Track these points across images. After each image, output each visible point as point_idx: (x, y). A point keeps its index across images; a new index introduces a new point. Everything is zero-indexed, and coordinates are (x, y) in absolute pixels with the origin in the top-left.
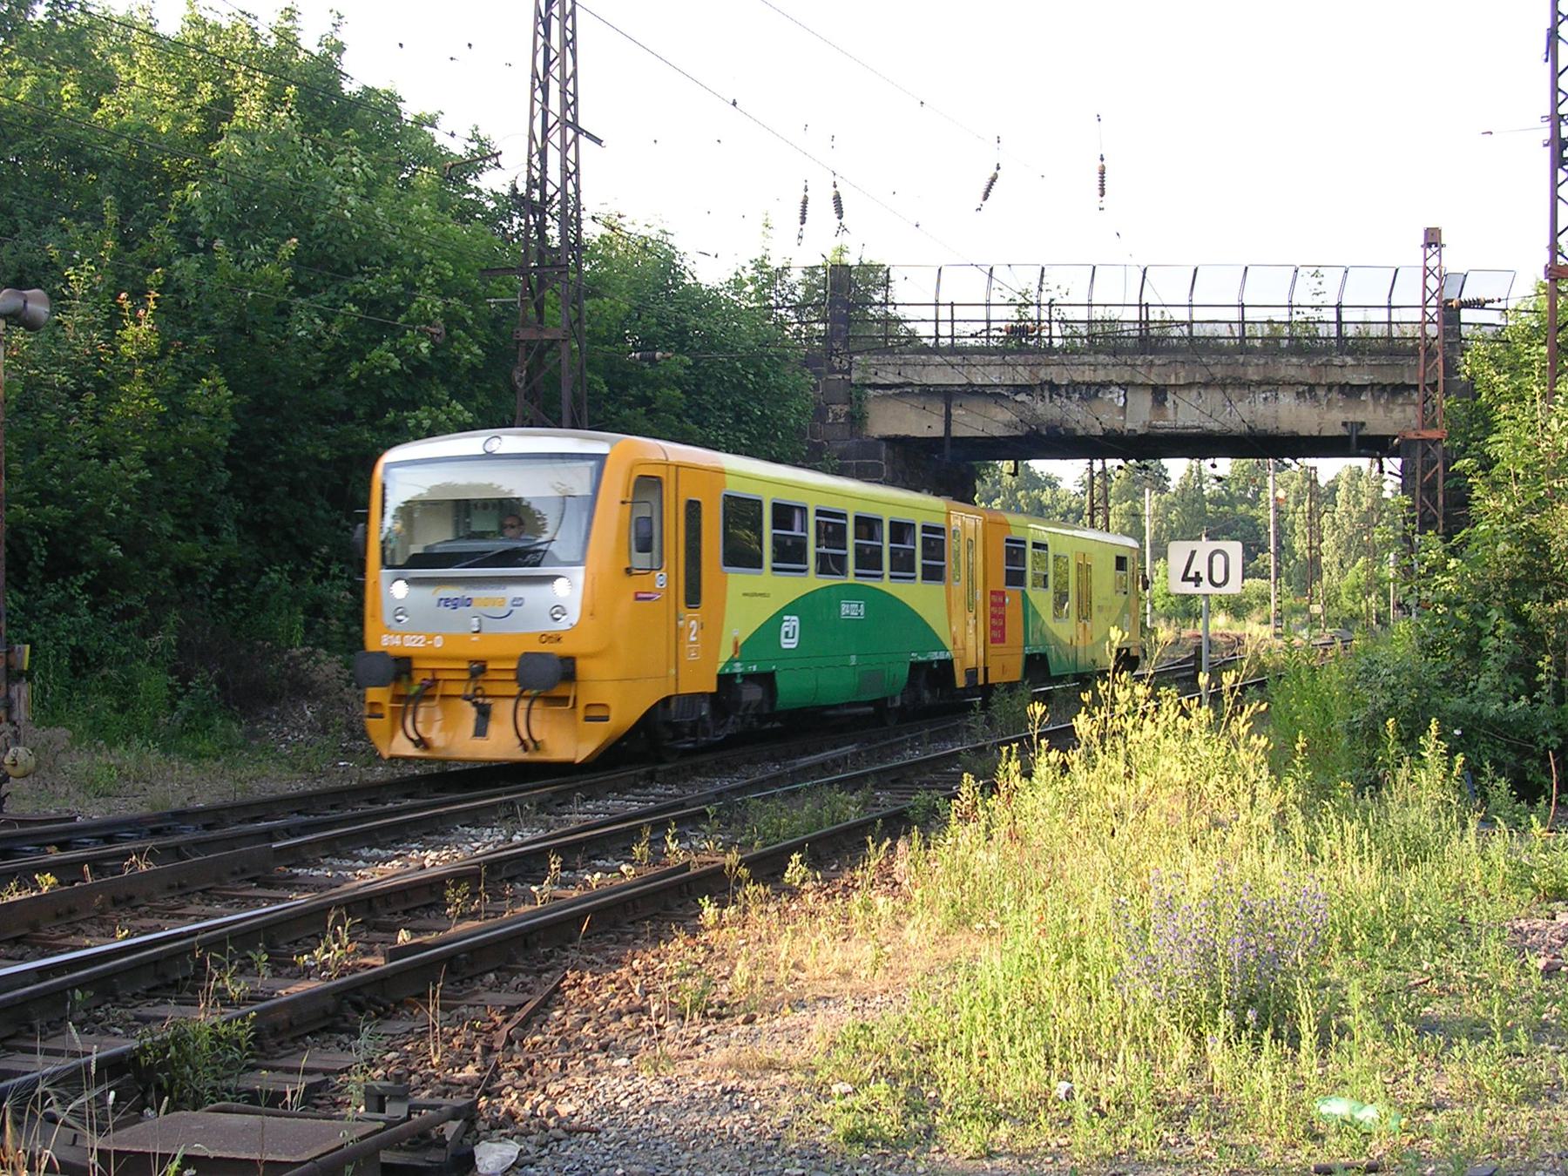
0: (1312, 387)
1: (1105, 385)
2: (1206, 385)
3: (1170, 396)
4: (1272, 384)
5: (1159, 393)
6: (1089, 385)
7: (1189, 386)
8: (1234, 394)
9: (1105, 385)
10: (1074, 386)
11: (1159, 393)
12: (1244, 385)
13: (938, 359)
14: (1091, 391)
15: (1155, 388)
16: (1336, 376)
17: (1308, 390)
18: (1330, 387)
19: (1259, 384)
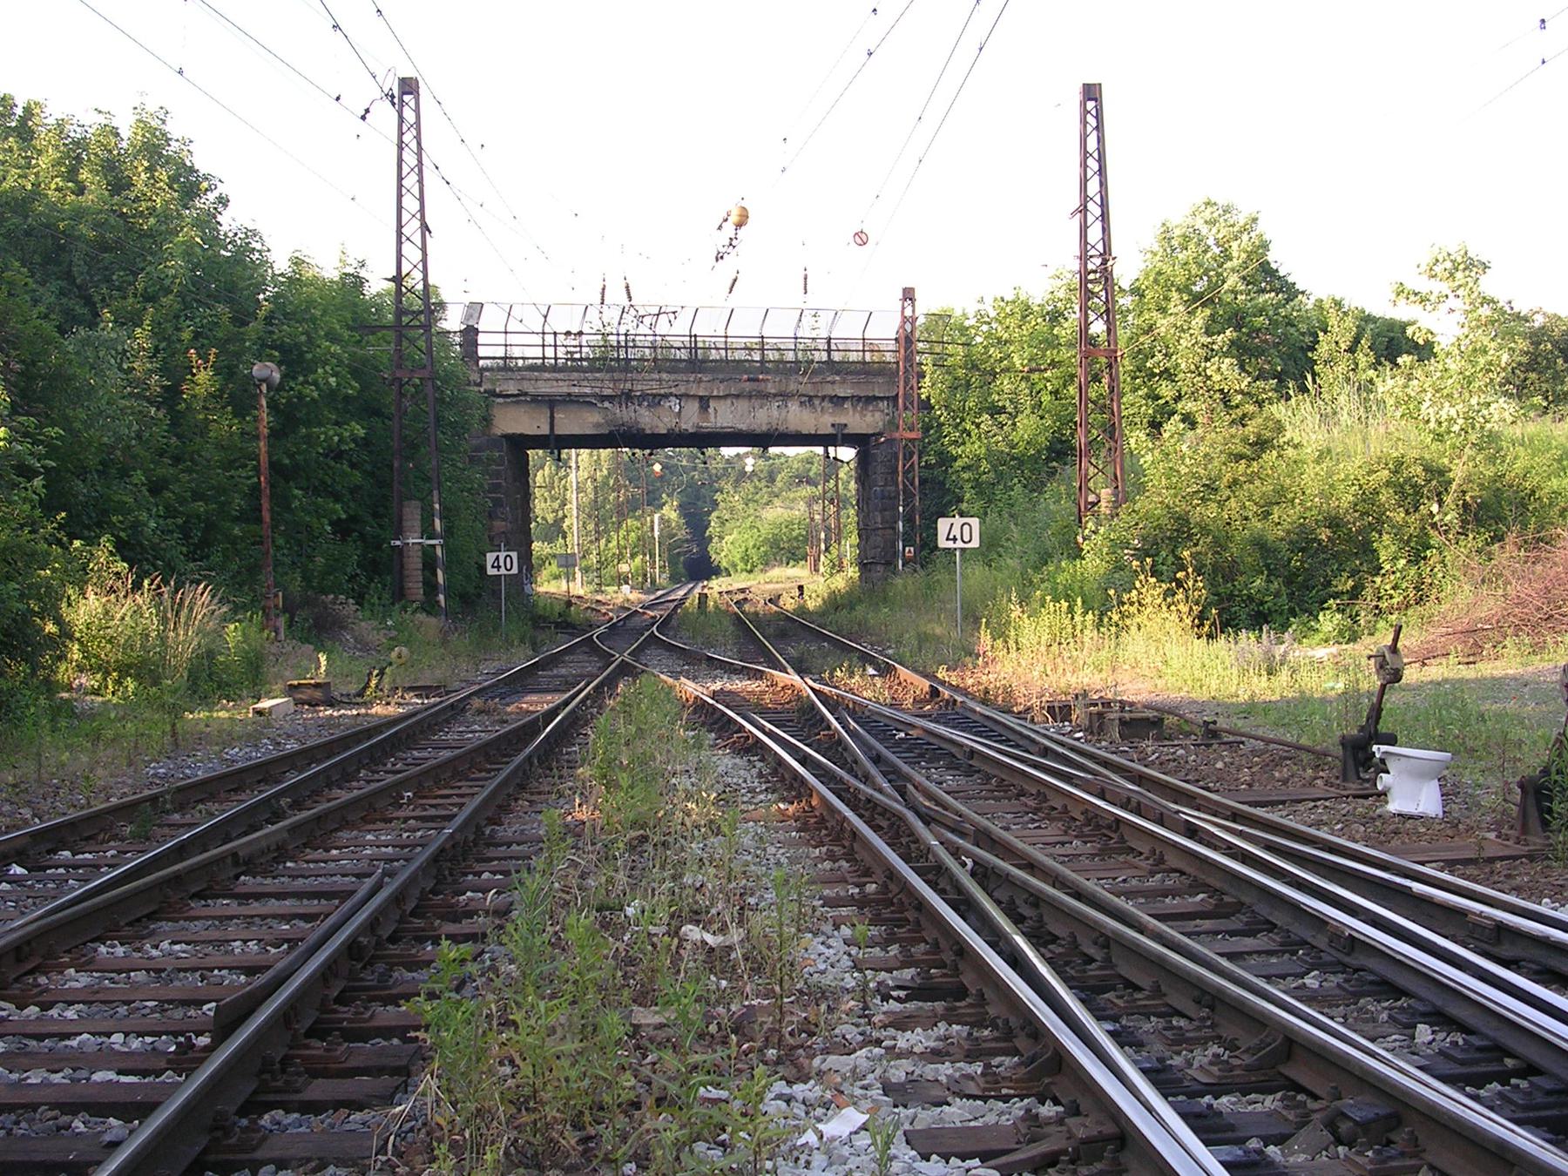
0: (811, 398)
1: (666, 396)
2: (737, 396)
3: (712, 404)
4: (784, 396)
5: (704, 402)
6: (654, 396)
7: (725, 397)
8: (757, 403)
9: (666, 396)
10: (644, 396)
11: (704, 402)
12: (765, 396)
13: (547, 375)
14: (656, 400)
15: (701, 398)
16: (829, 390)
17: (808, 400)
18: (823, 398)
19: (775, 395)
